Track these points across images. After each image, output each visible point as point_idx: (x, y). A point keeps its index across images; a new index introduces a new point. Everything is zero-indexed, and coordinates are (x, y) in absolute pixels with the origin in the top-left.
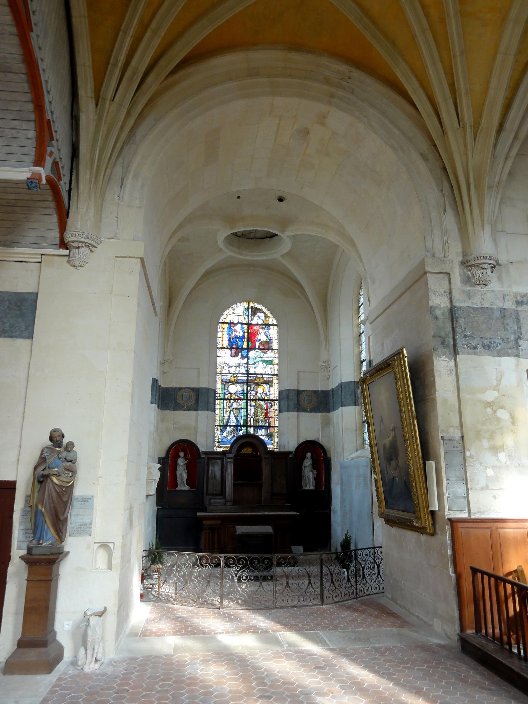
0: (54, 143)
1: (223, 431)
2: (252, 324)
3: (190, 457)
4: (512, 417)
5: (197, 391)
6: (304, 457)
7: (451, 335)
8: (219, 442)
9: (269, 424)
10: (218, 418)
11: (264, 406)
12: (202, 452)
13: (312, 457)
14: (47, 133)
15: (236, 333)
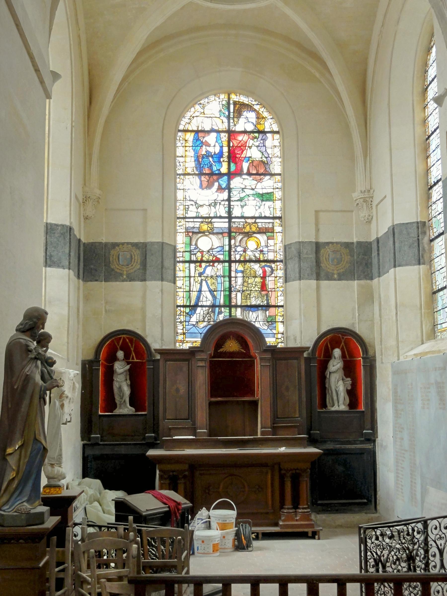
1: (189, 315)
2: (235, 132)
3: (135, 360)
5: (143, 248)
6: (328, 356)
8: (184, 334)
9: (268, 303)
10: (181, 294)
12: (156, 350)
13: (343, 356)
15: (208, 148)
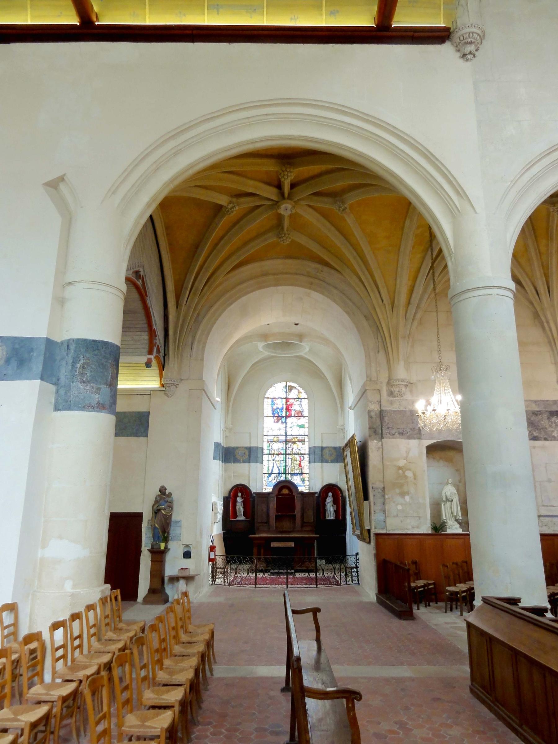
0: (157, 338)
1: (269, 477)
4: (415, 475)
5: (249, 449)
6: (327, 496)
7: (380, 427)
11: (298, 459)
13: (333, 496)
14: (153, 335)
